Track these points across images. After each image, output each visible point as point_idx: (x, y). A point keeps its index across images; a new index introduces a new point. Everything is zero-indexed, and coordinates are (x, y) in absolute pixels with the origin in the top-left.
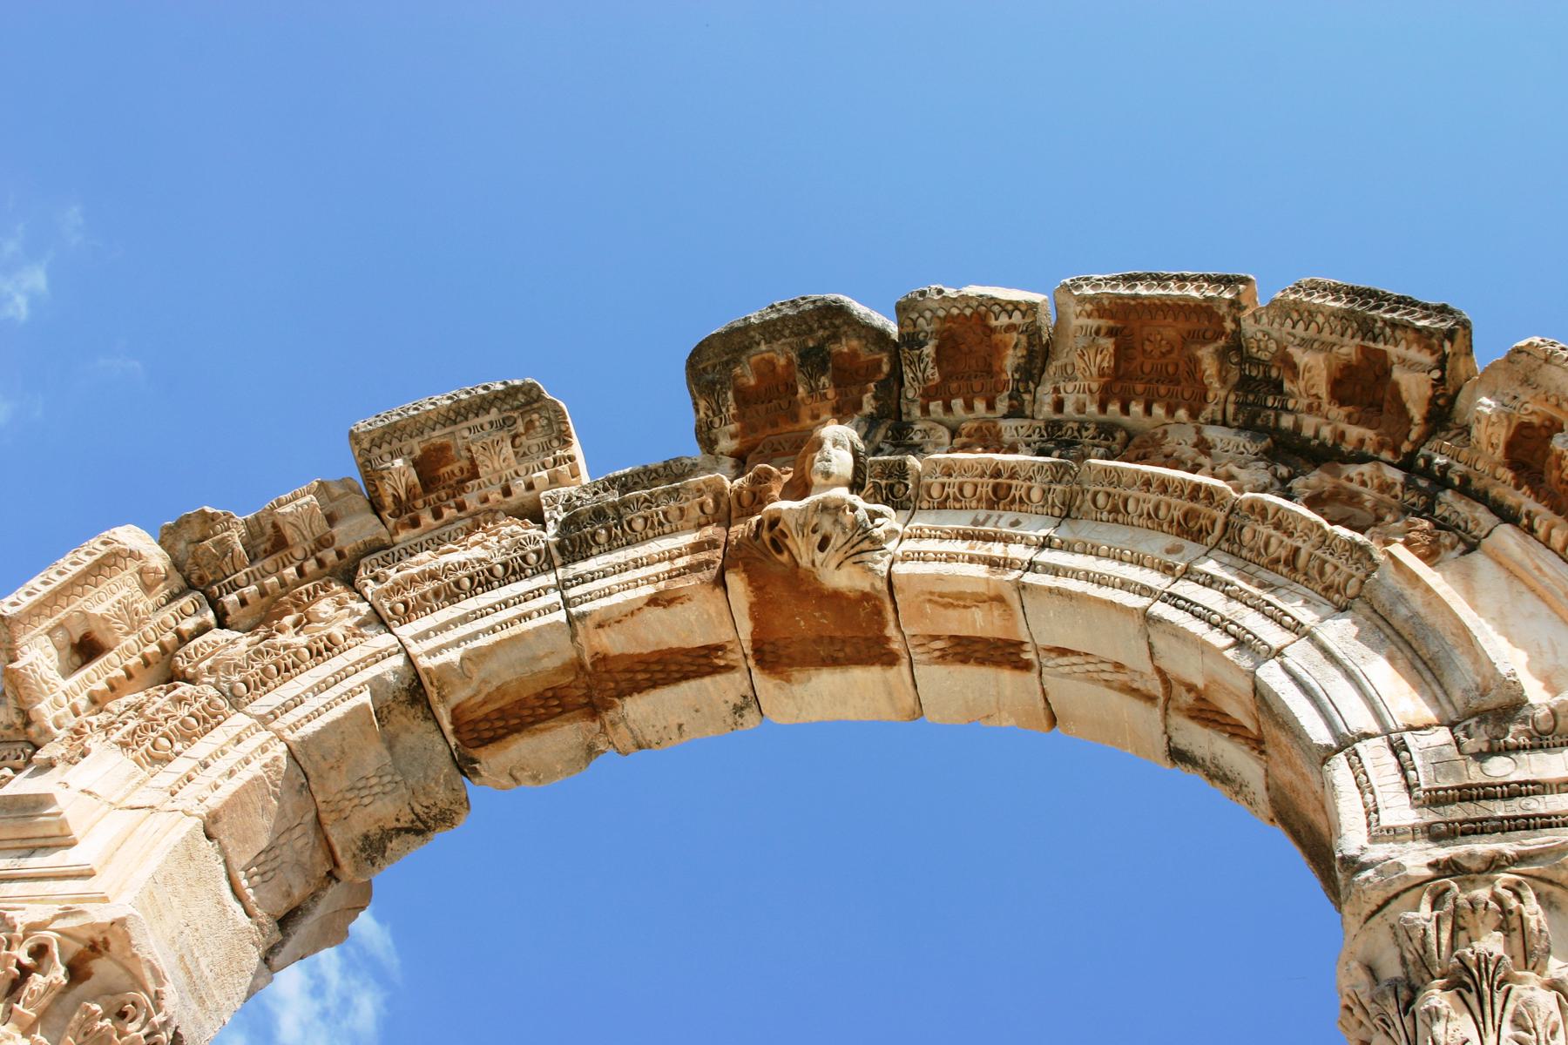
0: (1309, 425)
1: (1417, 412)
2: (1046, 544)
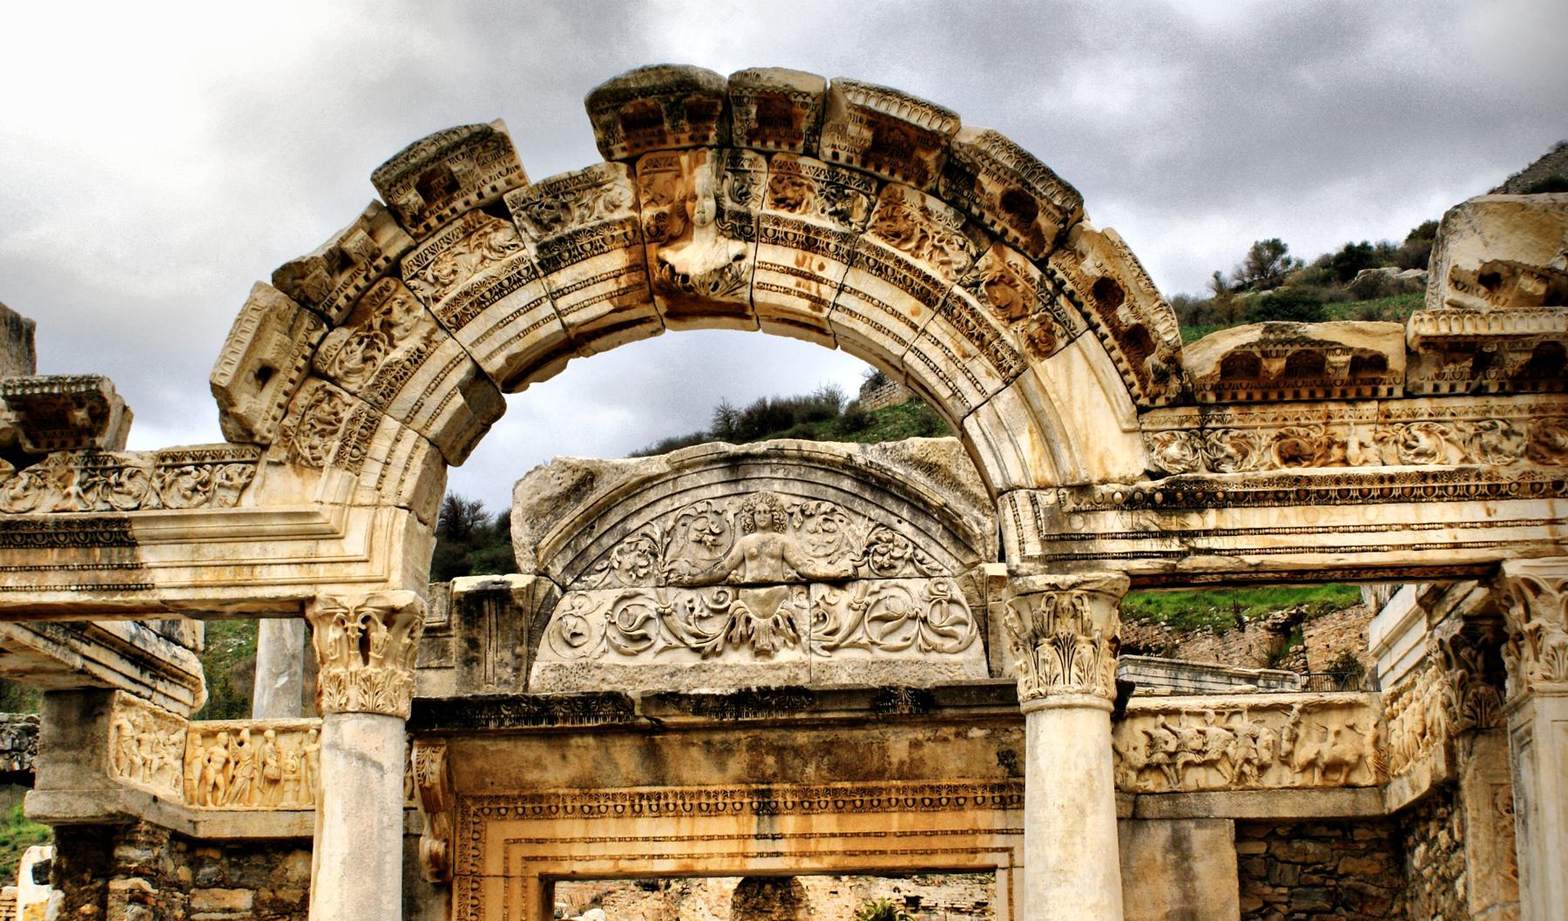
0: (988, 218)
1: (1049, 241)
2: (841, 289)
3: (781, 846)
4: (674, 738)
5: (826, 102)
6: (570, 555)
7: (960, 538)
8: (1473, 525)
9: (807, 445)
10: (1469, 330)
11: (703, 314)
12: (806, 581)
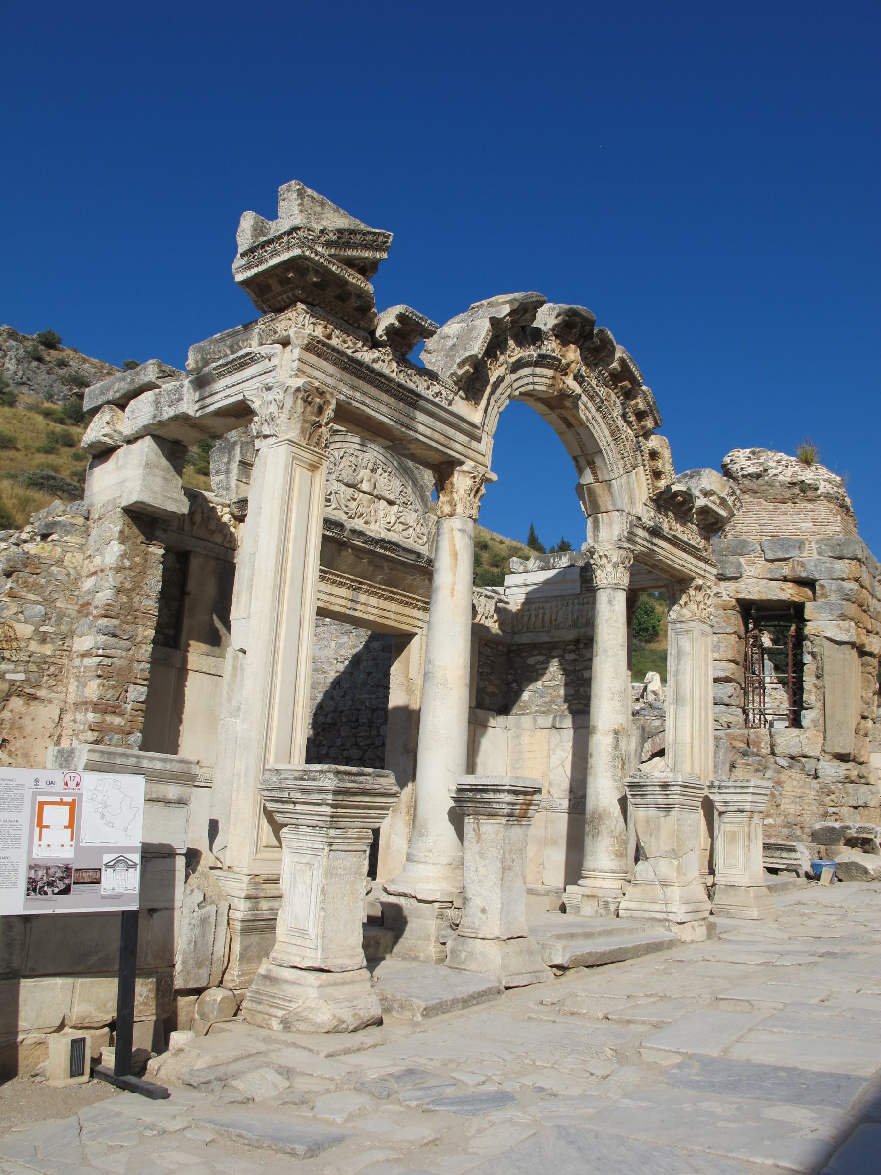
3: (359, 607)
12: (379, 498)
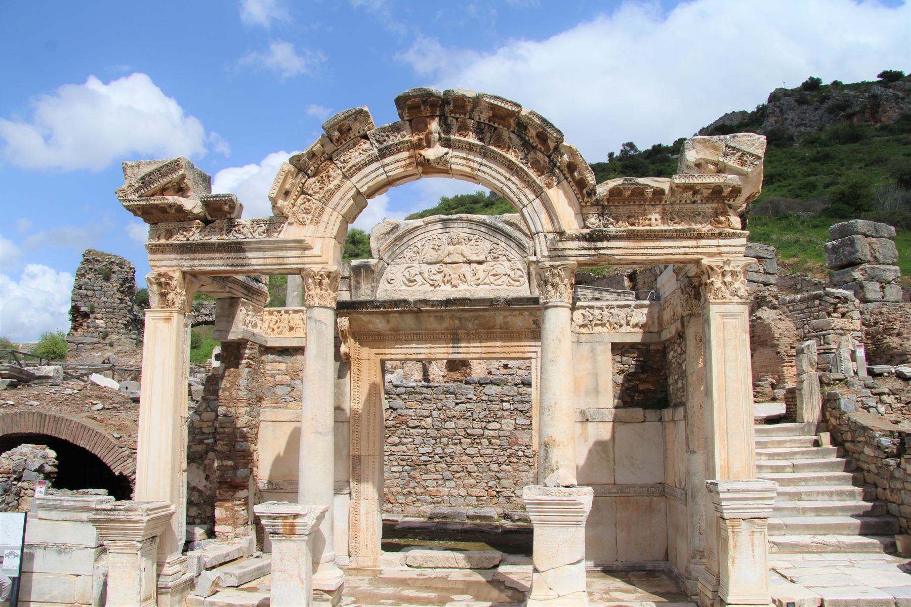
0: (531, 141)
2: (481, 164)
3: (460, 350)
4: (426, 315)
5: (477, 100)
6: (390, 253)
7: (521, 247)
8: (692, 247)
9: (470, 216)
10: (691, 181)
11: (434, 173)
12: (469, 262)
